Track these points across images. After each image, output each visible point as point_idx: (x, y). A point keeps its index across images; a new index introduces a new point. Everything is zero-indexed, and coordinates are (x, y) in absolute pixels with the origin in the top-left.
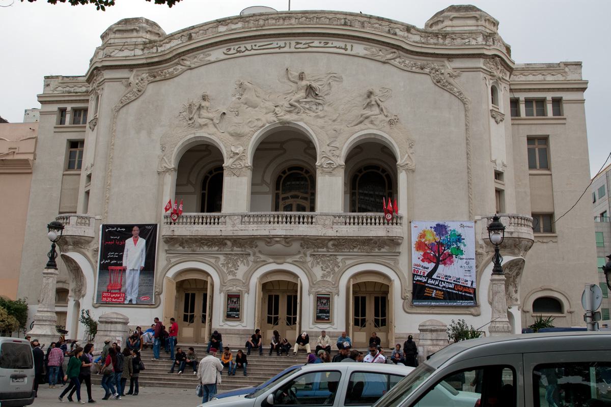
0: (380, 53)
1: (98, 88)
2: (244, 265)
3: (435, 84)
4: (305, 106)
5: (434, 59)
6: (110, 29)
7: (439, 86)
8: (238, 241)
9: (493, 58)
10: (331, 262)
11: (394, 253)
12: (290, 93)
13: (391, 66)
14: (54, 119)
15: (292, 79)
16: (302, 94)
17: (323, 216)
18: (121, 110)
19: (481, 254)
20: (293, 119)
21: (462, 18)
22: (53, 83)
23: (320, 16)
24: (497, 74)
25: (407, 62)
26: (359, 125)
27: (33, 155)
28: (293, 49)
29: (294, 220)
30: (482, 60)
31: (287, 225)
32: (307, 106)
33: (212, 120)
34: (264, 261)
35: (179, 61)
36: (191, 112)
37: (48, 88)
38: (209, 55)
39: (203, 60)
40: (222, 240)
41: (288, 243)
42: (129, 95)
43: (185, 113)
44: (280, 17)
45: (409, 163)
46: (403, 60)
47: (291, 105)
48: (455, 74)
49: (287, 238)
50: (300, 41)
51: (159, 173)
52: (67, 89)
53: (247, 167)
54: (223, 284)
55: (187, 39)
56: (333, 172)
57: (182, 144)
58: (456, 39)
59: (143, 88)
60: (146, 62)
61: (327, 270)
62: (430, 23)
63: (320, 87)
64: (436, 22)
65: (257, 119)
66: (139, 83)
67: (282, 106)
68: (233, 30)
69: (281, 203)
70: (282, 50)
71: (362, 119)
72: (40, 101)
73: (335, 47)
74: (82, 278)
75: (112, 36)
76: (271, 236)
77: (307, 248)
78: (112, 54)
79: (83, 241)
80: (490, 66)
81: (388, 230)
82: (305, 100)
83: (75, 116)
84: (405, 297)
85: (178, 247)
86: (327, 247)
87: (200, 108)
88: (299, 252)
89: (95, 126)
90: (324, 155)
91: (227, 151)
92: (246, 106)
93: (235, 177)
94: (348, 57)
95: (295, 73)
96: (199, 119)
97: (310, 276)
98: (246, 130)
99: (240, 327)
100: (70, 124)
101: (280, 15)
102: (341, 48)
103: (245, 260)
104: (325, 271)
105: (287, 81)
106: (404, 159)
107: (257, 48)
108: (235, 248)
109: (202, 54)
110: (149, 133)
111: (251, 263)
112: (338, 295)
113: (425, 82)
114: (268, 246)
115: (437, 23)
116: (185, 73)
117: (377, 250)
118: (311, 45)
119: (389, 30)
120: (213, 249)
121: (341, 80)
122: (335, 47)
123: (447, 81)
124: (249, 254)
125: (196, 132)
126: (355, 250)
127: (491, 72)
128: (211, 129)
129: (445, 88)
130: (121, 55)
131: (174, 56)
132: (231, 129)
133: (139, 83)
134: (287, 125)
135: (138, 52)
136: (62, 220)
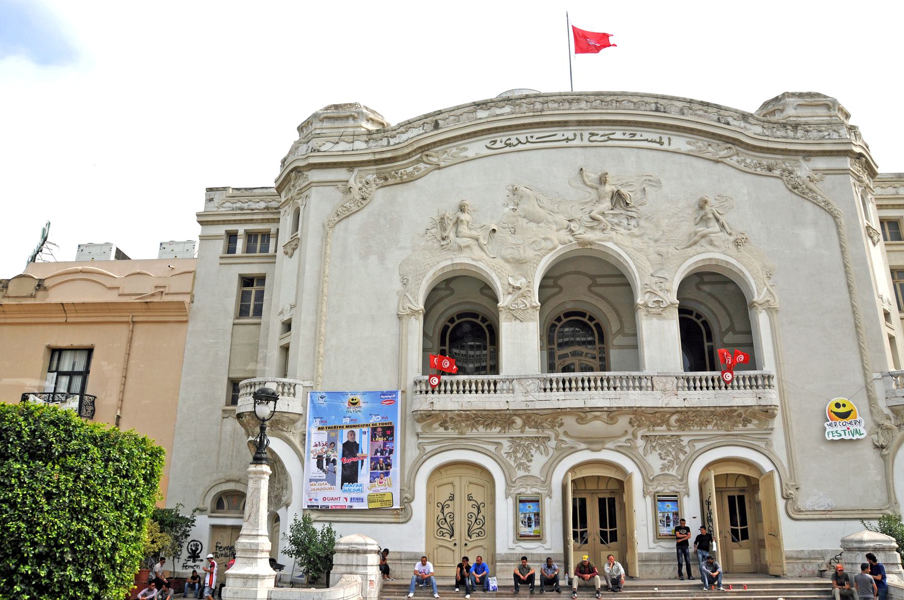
0: (710, 149)
1: (298, 197)
2: (541, 454)
3: (790, 191)
4: (613, 220)
5: (785, 157)
6: (315, 116)
7: (794, 192)
8: (533, 417)
9: (857, 158)
10: (673, 446)
11: (766, 429)
12: (588, 202)
13: (727, 167)
14: (220, 246)
15: (589, 183)
16: (606, 204)
17: (663, 378)
18: (337, 225)
19: (890, 429)
20: (597, 238)
21: (806, 105)
22: (218, 197)
23: (621, 99)
24: (865, 178)
25: (748, 161)
26: (694, 247)
27: (190, 296)
28: (586, 142)
29: (619, 385)
30: (849, 159)
31: (478, 395)
32: (615, 220)
33: (477, 240)
34: (573, 448)
35: (421, 157)
36: (444, 229)
37: (211, 204)
38: (465, 149)
39: (457, 156)
40: (508, 416)
41: (612, 419)
42: (348, 204)
43: (434, 230)
44: (564, 100)
45: (768, 298)
46: (742, 158)
47: (593, 219)
48: (815, 176)
49: (611, 412)
50: (596, 132)
51: (400, 317)
52: (239, 205)
53: (534, 307)
54: (509, 484)
55: (432, 128)
56: (664, 314)
57: (434, 274)
58: (810, 131)
59: (369, 194)
60: (373, 158)
61: (670, 458)
62: (765, 112)
63: (630, 194)
64: (772, 112)
65: (544, 239)
66: (364, 188)
67: (579, 220)
68: (498, 115)
69: (557, 362)
70: (570, 143)
71: (696, 238)
72: (198, 222)
73: (647, 140)
74: (281, 476)
75: (319, 125)
76: (588, 410)
77: (639, 426)
78: (322, 149)
79: (285, 419)
80: (856, 168)
81: (758, 396)
82: (612, 212)
83: (248, 242)
84: (787, 496)
85: (437, 429)
86: (668, 425)
87: (458, 222)
89: (294, 249)
90: (648, 290)
91: (503, 284)
92: (525, 221)
93: (518, 322)
94: (665, 153)
95: (592, 176)
96: (457, 238)
97: (643, 468)
98: (530, 254)
99: (541, 551)
100: (243, 253)
101: (565, 97)
102: (655, 142)
103: (541, 447)
104: (665, 459)
105: (581, 185)
106: (763, 294)
107: (534, 140)
109: (455, 148)
110: (382, 258)
111: (551, 452)
112: (688, 496)
113: (774, 188)
114: (582, 424)
115: (773, 113)
116: (431, 174)
117: (740, 425)
118: (611, 137)
119: (719, 119)
120: (493, 430)
121: (660, 184)
122: (647, 140)
123: (807, 187)
124: (548, 439)
125: (453, 256)
126: (710, 427)
127: (859, 177)
128: (478, 253)
129: (805, 196)
130: (331, 149)
131: (415, 151)
132: (507, 253)
133: (364, 188)
134: (589, 247)
135: (360, 145)
136: (249, 388)
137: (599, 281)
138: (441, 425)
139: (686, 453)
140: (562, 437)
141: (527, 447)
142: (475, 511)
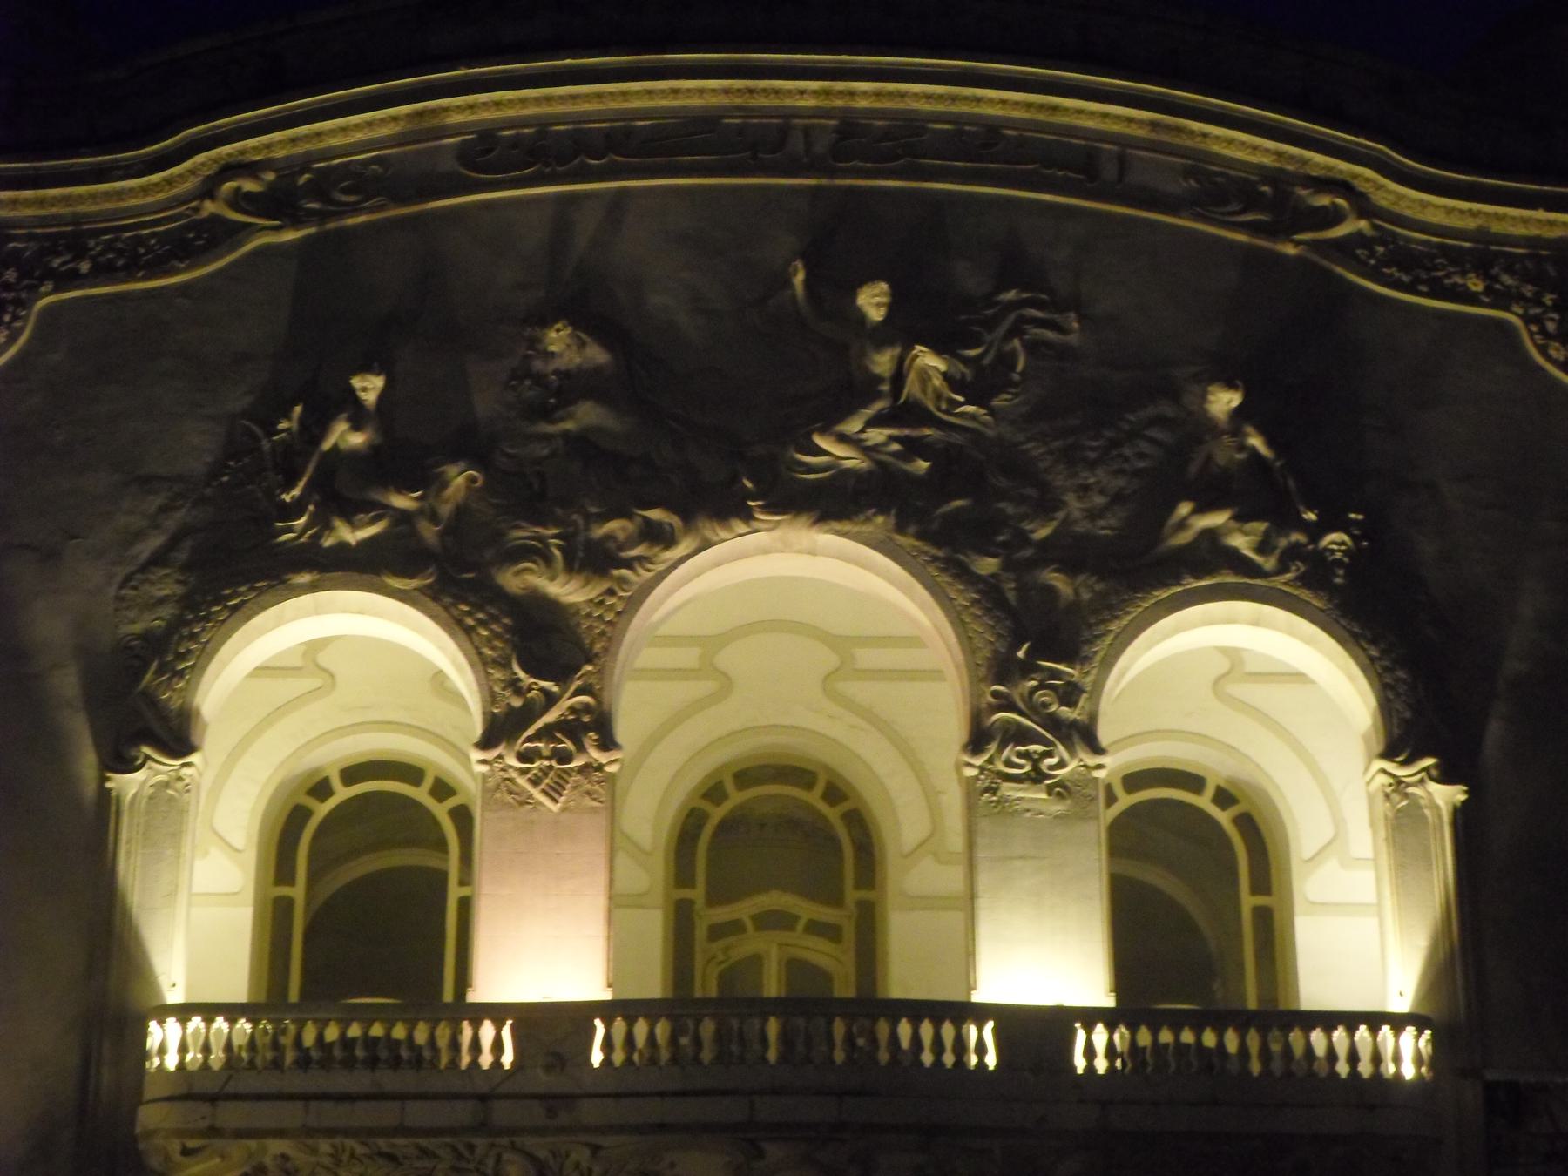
137: (868, 658)
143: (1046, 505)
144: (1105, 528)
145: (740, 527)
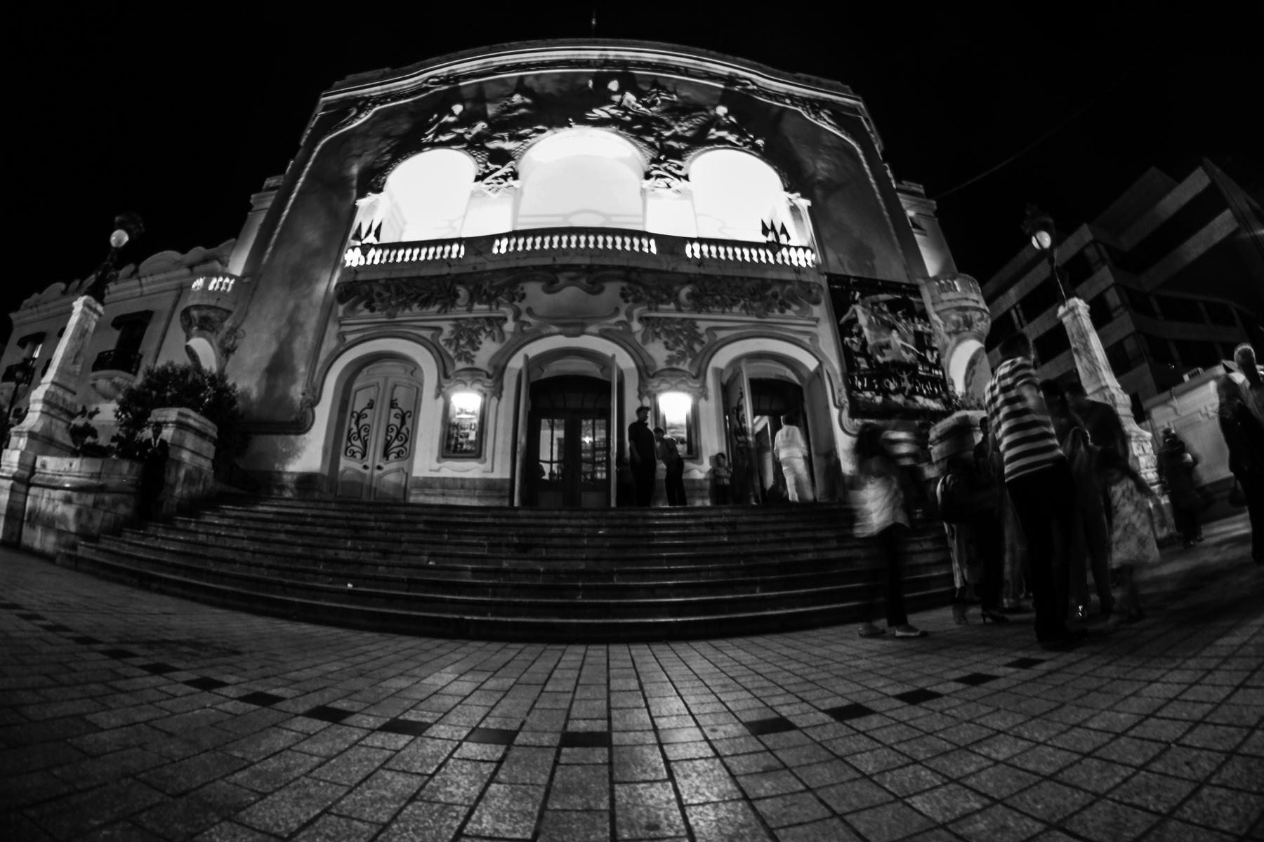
10: (685, 333)
11: (809, 319)
61: (678, 348)
77: (637, 301)
85: (361, 311)
88: (617, 311)
103: (496, 332)
108: (477, 306)
117: (776, 311)
124: (505, 319)
126: (736, 309)
138: (367, 306)
139: (703, 342)
140: (525, 317)
141: (477, 333)
142: (397, 422)
143: (669, 128)
144: (688, 134)
145: (567, 128)
